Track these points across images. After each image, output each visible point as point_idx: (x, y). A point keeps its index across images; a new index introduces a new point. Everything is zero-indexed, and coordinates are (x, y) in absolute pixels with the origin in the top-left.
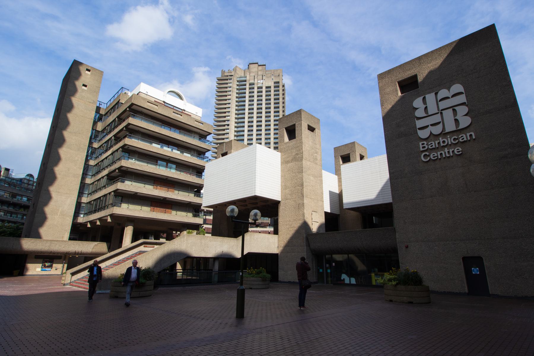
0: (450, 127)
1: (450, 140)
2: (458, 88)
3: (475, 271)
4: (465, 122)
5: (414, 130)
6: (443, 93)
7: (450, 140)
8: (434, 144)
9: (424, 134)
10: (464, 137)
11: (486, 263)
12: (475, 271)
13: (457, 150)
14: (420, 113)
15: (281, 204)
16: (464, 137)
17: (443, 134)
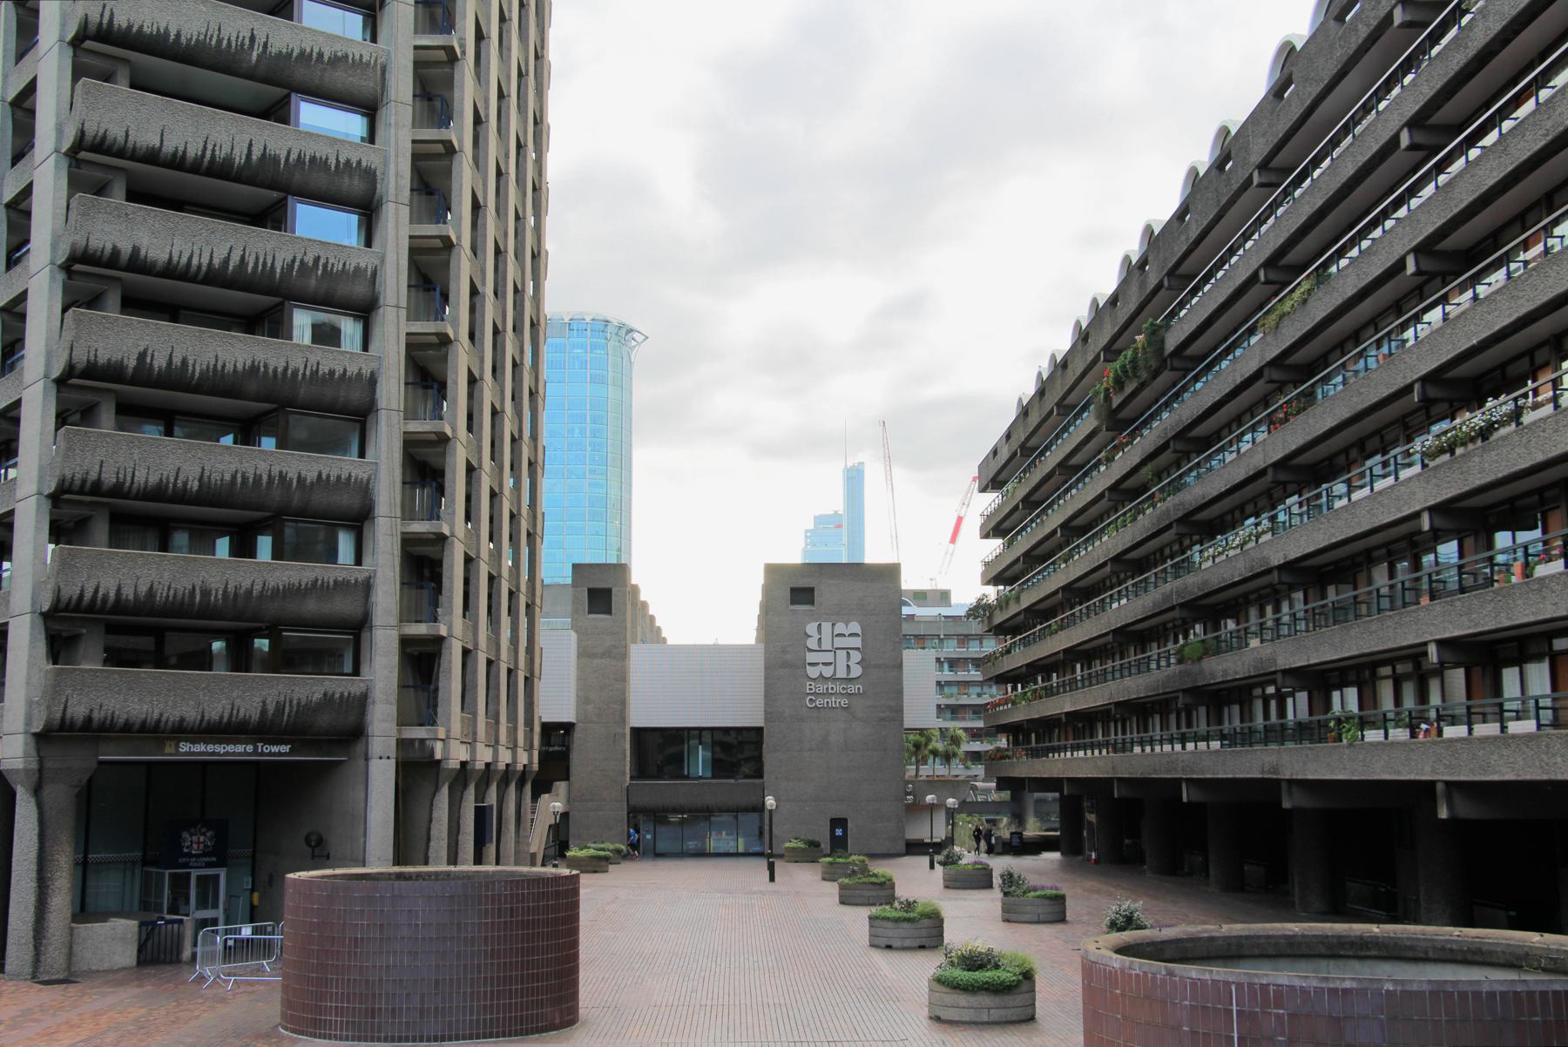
0: (842, 673)
1: (838, 688)
2: (855, 627)
3: (839, 832)
4: (856, 671)
5: (804, 664)
6: (840, 628)
7: (838, 688)
8: (822, 688)
9: (813, 672)
10: (853, 689)
11: (849, 825)
12: (839, 832)
13: (844, 702)
14: (812, 643)
15: (577, 729)
16: (853, 689)
17: (833, 679)
